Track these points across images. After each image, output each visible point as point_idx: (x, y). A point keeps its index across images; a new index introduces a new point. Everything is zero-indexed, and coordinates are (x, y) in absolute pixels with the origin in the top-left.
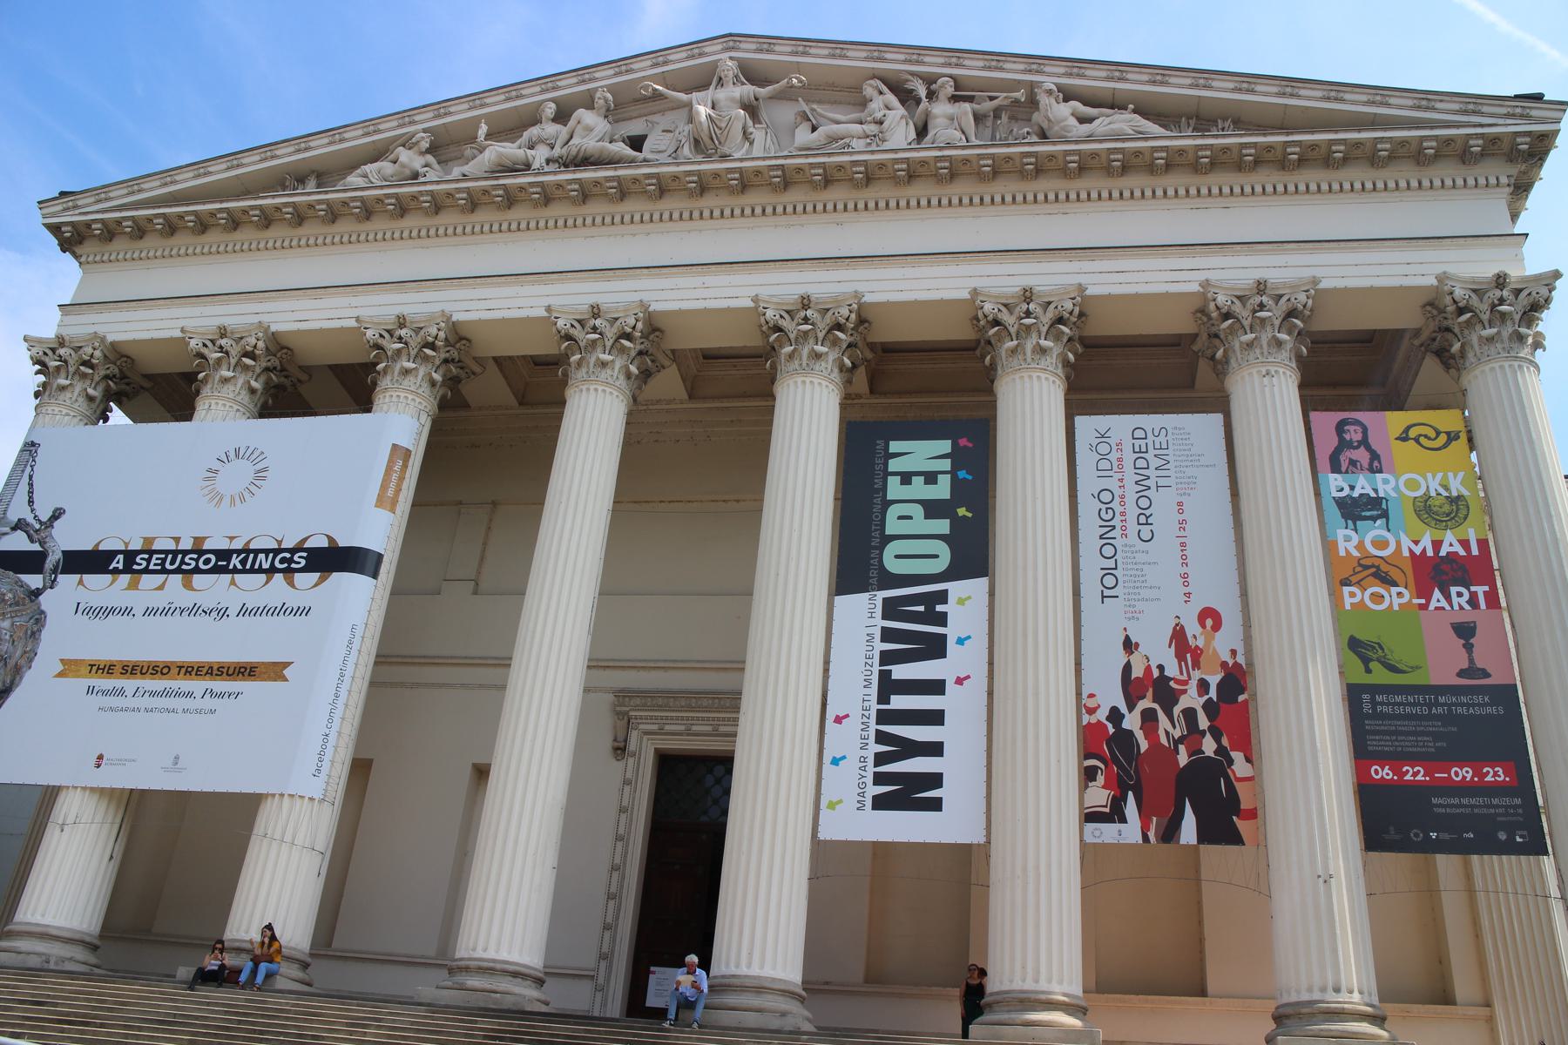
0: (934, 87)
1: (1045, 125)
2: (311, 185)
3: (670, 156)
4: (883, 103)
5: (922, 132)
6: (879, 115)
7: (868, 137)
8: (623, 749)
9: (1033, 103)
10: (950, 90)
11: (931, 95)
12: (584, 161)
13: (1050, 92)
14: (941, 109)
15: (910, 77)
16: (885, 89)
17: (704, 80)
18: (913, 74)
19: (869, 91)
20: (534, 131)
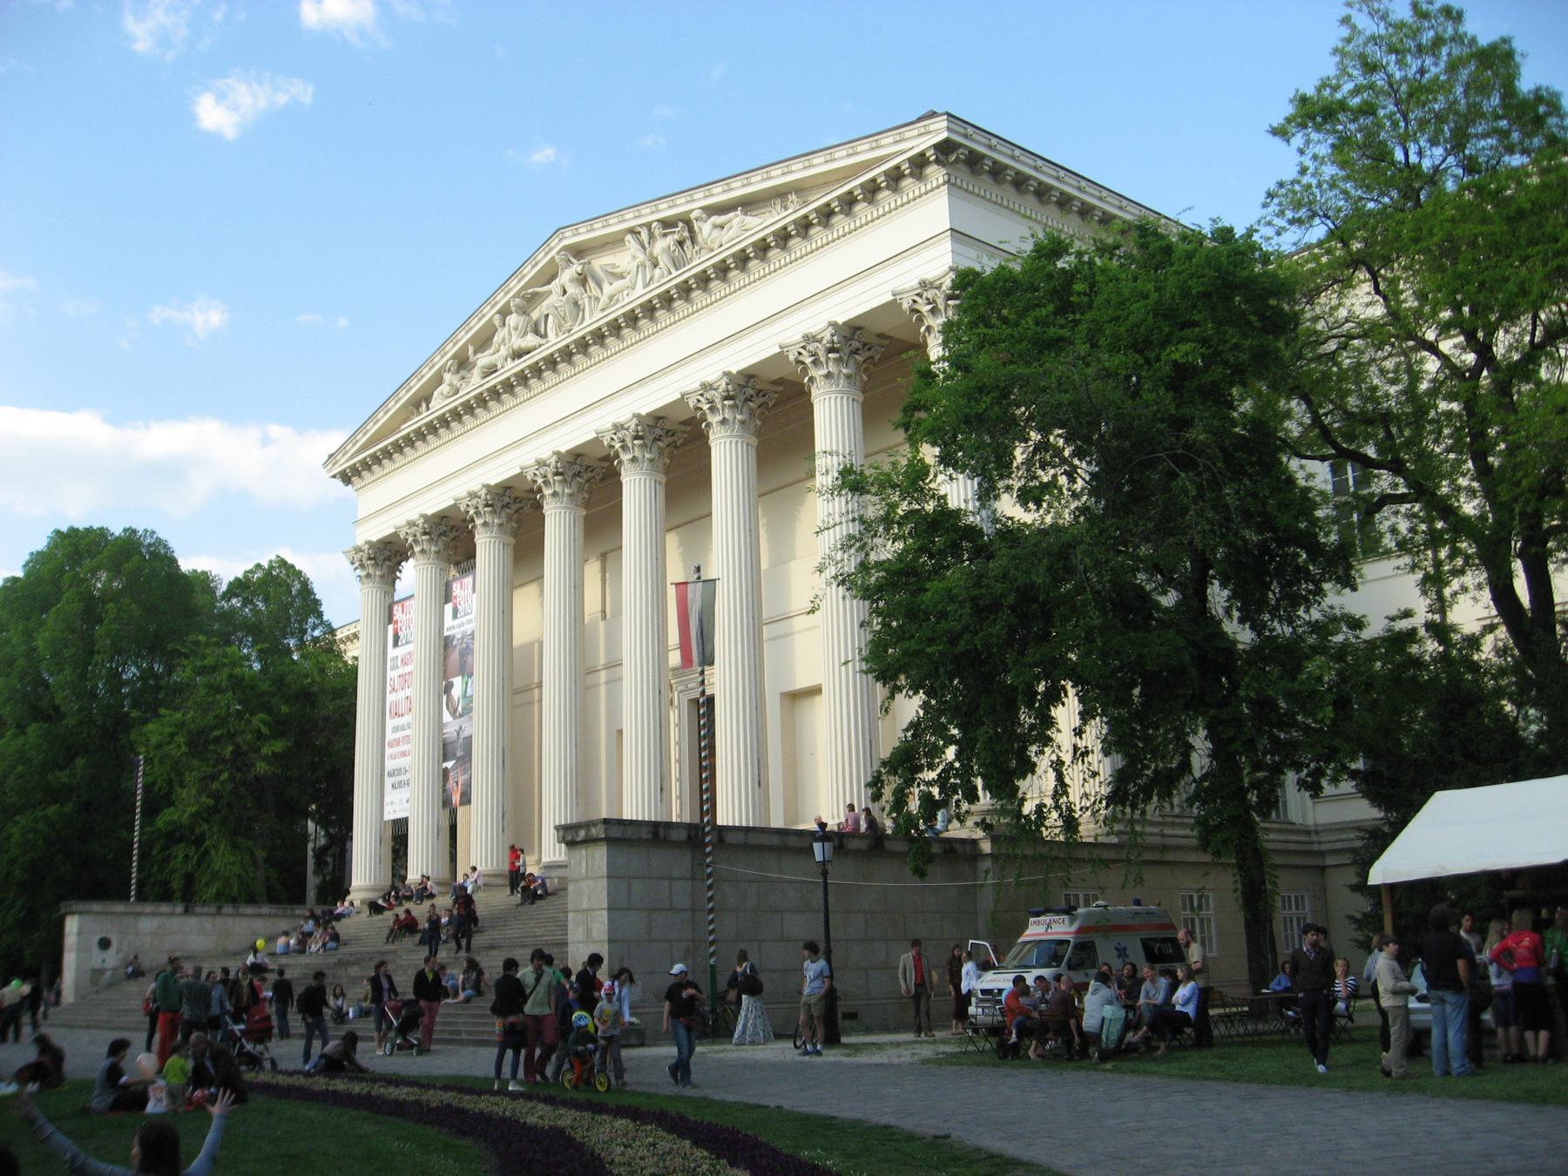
11: (651, 236)
12: (518, 354)
14: (661, 245)
18: (641, 226)
20: (496, 339)
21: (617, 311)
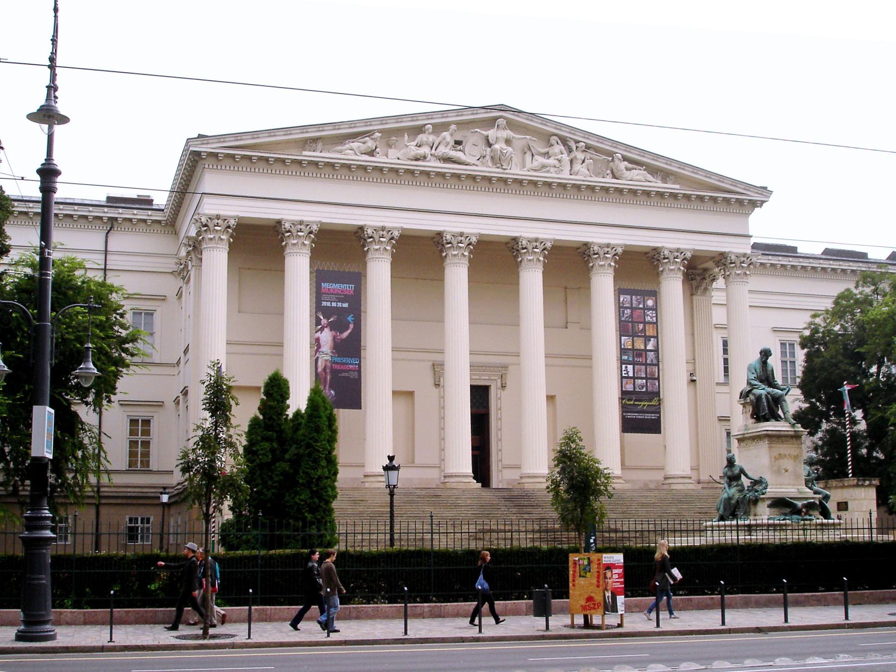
0: (577, 144)
1: (615, 171)
2: (320, 145)
3: (478, 160)
4: (558, 148)
5: (571, 161)
6: (559, 157)
7: (555, 167)
8: (439, 385)
9: (613, 160)
10: (584, 148)
11: (577, 147)
12: (448, 160)
13: (620, 159)
14: (580, 156)
15: (570, 140)
16: (559, 142)
17: (491, 123)
18: (570, 138)
19: (554, 139)
20: (422, 137)
21: (541, 176)
